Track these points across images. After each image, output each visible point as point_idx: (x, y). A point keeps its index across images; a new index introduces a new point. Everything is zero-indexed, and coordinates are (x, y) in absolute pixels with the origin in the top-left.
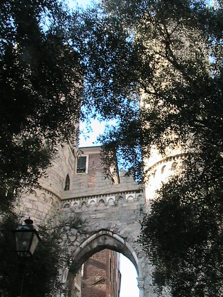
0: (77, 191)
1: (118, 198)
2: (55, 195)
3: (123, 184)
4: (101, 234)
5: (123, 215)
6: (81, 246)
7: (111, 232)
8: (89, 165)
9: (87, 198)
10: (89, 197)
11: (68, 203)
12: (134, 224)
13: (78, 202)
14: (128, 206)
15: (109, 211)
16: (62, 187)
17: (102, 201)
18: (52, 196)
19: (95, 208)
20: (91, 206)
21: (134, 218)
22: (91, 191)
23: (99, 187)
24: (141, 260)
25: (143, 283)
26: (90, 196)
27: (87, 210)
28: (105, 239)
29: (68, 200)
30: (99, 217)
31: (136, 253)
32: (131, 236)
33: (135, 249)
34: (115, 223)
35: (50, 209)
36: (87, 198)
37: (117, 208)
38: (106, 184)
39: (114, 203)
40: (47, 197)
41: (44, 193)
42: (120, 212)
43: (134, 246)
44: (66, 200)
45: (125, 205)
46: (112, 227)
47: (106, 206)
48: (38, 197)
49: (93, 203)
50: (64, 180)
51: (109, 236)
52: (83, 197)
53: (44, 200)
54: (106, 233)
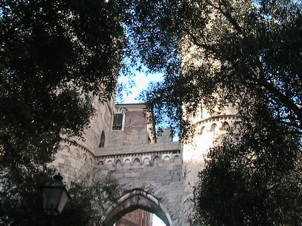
0: (112, 149)
2: (89, 151)
3: (159, 144)
7: (145, 192)
8: (126, 122)
9: (122, 156)
10: (124, 155)
13: (113, 159)
15: (144, 170)
16: (97, 144)
17: (137, 160)
18: (85, 153)
19: (129, 167)
20: (125, 165)
22: (127, 149)
23: (135, 145)
26: (125, 154)
27: (121, 168)
28: (139, 198)
29: (103, 157)
30: (133, 176)
31: (170, 214)
32: (166, 197)
33: (169, 210)
34: (149, 183)
35: (83, 166)
36: (122, 156)
37: (153, 168)
40: (80, 153)
41: (78, 148)
43: (169, 208)
44: (100, 157)
47: (141, 165)
48: (71, 153)
49: (128, 162)
50: (99, 136)
51: (143, 195)
52: (118, 155)
53: (77, 156)
54: (140, 192)
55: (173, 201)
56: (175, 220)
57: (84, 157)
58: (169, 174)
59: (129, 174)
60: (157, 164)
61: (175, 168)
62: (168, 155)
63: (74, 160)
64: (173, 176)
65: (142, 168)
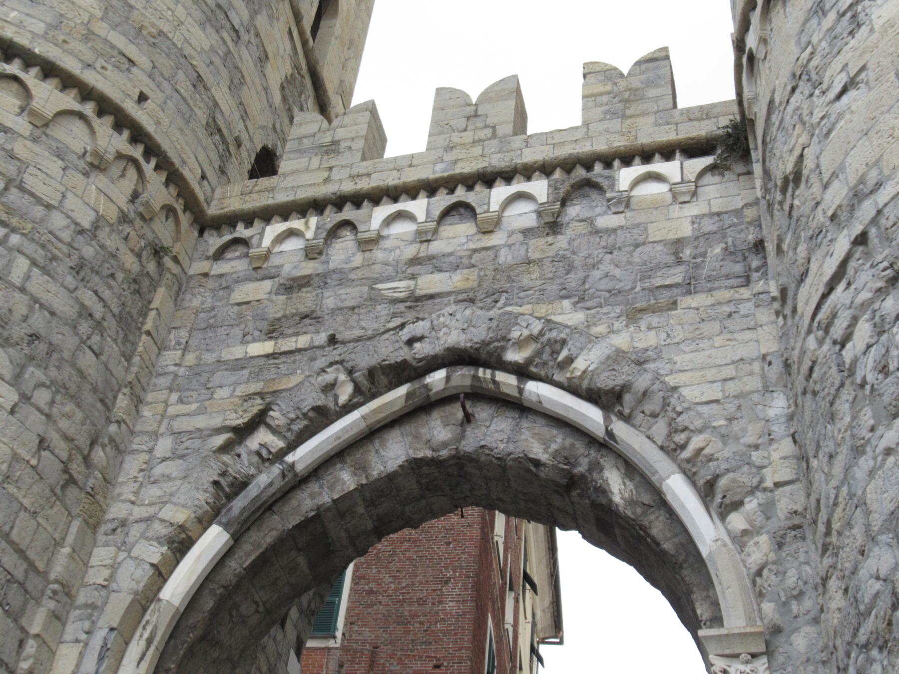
1: (564, 188)
2: (164, 164)
4: (440, 386)
5: (596, 274)
6: (290, 458)
11: (241, 231)
12: (673, 312)
14: (637, 226)
15: (505, 257)
19: (410, 251)
20: (386, 244)
21: (678, 279)
23: (450, 148)
24: (737, 521)
27: (358, 259)
28: (468, 418)
29: (248, 218)
31: (691, 478)
32: (657, 377)
33: (686, 454)
37: (561, 241)
38: (494, 135)
39: (539, 214)
42: (578, 260)
43: (680, 438)
44: (231, 220)
45: (607, 221)
46: (515, 334)
48: (42, 125)
49: (402, 228)
52: (339, 202)
54: (475, 377)
55: (715, 392)
56: (737, 505)
57: (123, 175)
58: (671, 259)
59: (411, 283)
60: (590, 221)
61: (709, 226)
62: (658, 166)
63: (55, 166)
64: (697, 266)
65: (486, 249)
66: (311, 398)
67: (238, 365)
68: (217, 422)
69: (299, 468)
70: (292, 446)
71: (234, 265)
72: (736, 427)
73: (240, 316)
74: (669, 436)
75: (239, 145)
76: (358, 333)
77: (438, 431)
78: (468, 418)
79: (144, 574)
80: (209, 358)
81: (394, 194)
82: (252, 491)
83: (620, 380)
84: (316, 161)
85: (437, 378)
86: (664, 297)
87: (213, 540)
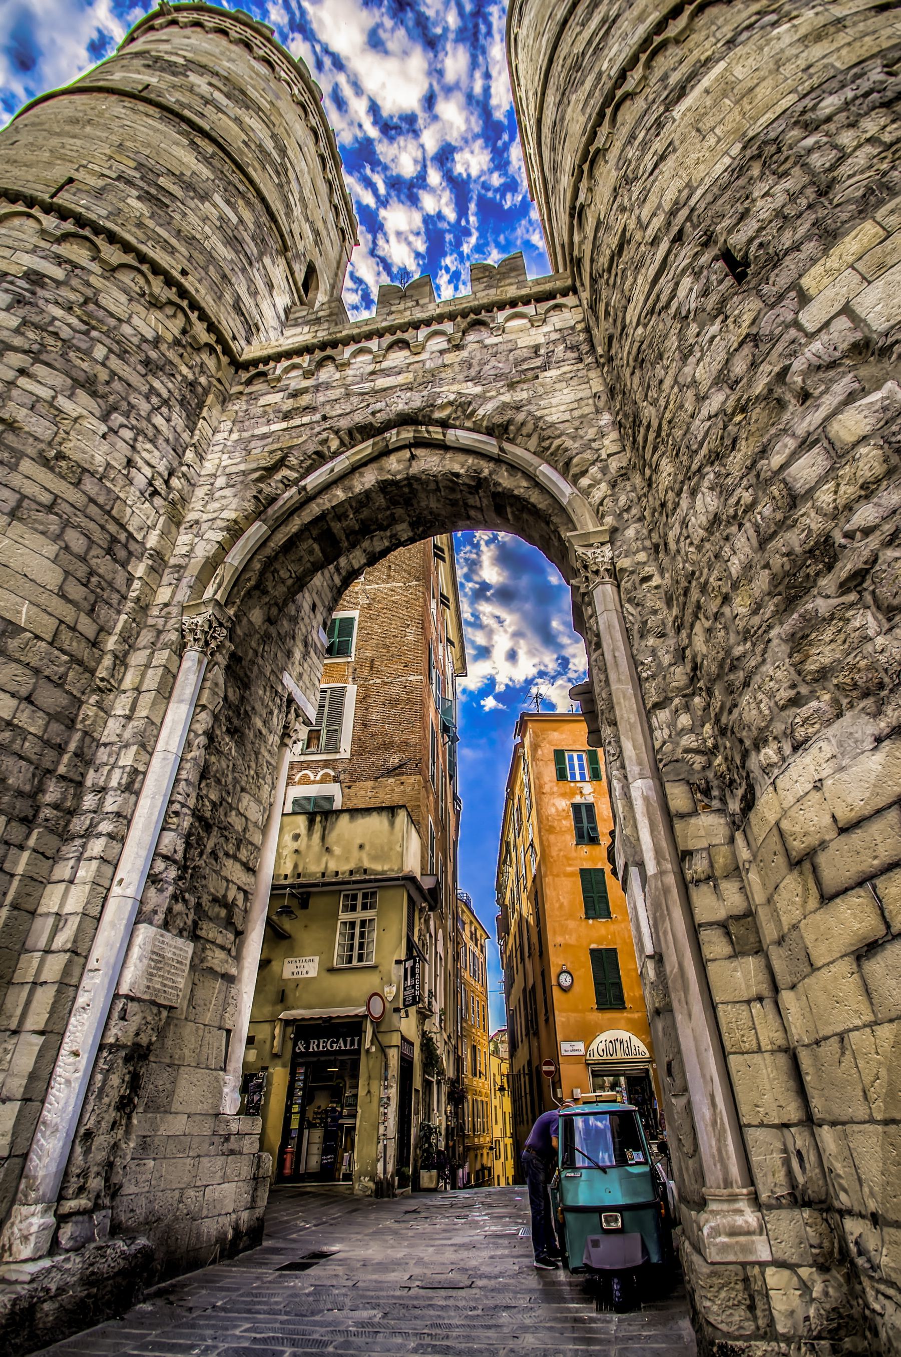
4: (394, 439)
5: (487, 367)
6: (302, 483)
13: (305, 361)
15: (429, 365)
19: (371, 368)
24: (585, 482)
25: (610, 554)
27: (337, 375)
28: (413, 457)
29: (266, 360)
32: (529, 413)
37: (464, 354)
39: (449, 341)
42: (474, 362)
43: (546, 444)
44: (255, 362)
46: (439, 402)
55: (567, 416)
56: (584, 473)
61: (555, 336)
66: (311, 448)
67: (264, 436)
68: (254, 466)
69: (309, 488)
70: (303, 477)
71: (259, 386)
72: (581, 432)
73: (265, 412)
74: (539, 445)
75: (258, 330)
76: (340, 412)
77: (394, 465)
78: (413, 457)
79: (212, 548)
80: (246, 435)
81: (355, 339)
82: (280, 502)
83: (506, 418)
84: (306, 329)
85: (392, 436)
86: (530, 374)
87: (256, 530)
